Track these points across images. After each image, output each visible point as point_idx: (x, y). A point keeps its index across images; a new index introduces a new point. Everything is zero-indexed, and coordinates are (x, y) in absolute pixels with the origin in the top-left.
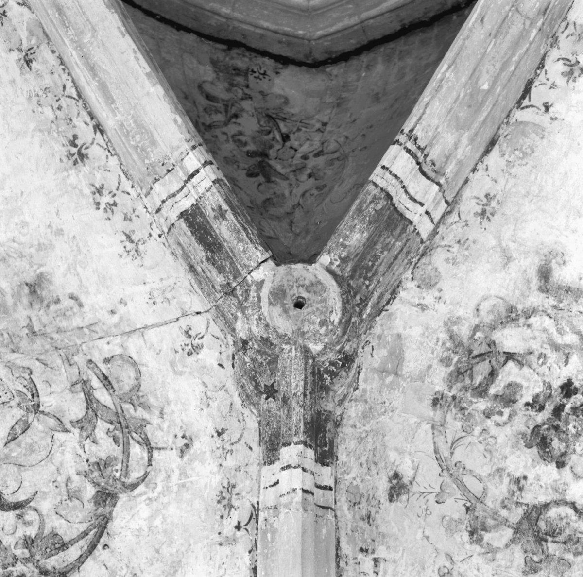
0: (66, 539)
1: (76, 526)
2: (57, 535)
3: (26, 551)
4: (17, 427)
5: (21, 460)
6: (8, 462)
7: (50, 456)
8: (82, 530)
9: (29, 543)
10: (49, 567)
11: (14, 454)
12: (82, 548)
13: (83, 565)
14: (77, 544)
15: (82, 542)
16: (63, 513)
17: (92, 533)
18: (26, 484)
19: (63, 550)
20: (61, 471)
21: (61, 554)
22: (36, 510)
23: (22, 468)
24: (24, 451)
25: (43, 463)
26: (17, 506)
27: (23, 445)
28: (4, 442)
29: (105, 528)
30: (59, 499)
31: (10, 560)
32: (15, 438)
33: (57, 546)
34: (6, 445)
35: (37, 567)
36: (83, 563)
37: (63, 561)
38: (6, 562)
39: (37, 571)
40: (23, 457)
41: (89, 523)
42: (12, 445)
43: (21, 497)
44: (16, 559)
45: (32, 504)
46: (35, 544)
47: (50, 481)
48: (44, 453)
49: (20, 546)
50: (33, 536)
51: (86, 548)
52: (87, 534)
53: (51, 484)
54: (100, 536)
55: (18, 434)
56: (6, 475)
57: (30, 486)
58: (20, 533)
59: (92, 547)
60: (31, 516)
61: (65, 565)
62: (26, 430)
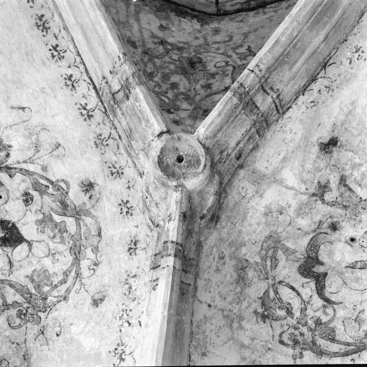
0: (337, 338)
1: (347, 336)
2: (335, 332)
3: (314, 325)
4: (359, 263)
5: (348, 281)
6: (341, 276)
7: (364, 291)
8: (348, 341)
9: (318, 322)
10: (318, 343)
11: (346, 275)
12: (341, 349)
13: (334, 358)
14: (340, 345)
15: (343, 347)
16: (346, 325)
17: (352, 347)
18: (340, 294)
19: (331, 342)
20: (363, 304)
21: (329, 342)
22: (335, 310)
23: (345, 285)
24: (353, 278)
25: (357, 292)
26: (328, 301)
27: (355, 275)
28: (347, 265)
29: (361, 351)
30: (350, 316)
31: (303, 322)
32: (353, 268)
33: (330, 337)
34: (346, 267)
35: (313, 337)
36: (335, 357)
37: (327, 347)
38: (301, 321)
39: (311, 339)
40: (350, 281)
41: (354, 341)
42: (350, 270)
43: (333, 299)
44: (306, 324)
45: (335, 306)
46: (321, 326)
47: (353, 303)
48: (361, 288)
49: (313, 320)
50: (323, 321)
51: (343, 351)
52: (349, 346)
53: (352, 305)
54: (354, 353)
55: (357, 267)
56: (335, 282)
57: (342, 297)
58: (318, 314)
59: (346, 354)
60: (330, 311)
61: (326, 349)
62: (362, 269)
